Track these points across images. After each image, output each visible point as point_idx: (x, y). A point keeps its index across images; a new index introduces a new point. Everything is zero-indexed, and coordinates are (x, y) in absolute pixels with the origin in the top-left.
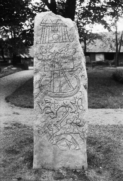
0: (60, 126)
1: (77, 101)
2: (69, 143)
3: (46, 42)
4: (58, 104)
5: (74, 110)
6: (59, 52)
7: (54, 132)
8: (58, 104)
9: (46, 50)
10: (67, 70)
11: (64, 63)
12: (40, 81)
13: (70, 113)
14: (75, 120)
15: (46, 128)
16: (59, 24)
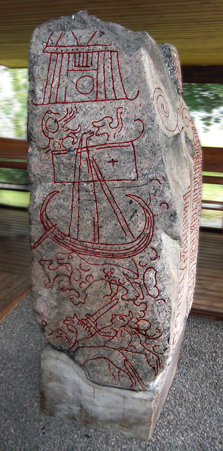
0: (94, 326)
1: (141, 273)
2: (117, 370)
3: (58, 100)
4: (89, 273)
5: (132, 295)
6: (95, 130)
7: (80, 336)
8: (89, 273)
9: (56, 121)
10: (118, 184)
11: (108, 162)
12: (44, 207)
13: (120, 300)
14: (134, 320)
15: (61, 324)
16: (95, 45)
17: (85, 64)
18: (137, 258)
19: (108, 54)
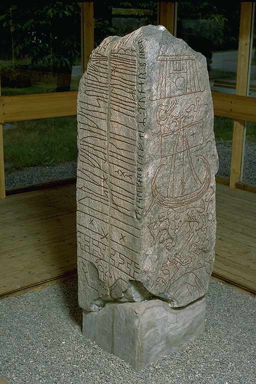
0: (179, 261)
17: (179, 69)
18: (204, 198)
19: (191, 61)
